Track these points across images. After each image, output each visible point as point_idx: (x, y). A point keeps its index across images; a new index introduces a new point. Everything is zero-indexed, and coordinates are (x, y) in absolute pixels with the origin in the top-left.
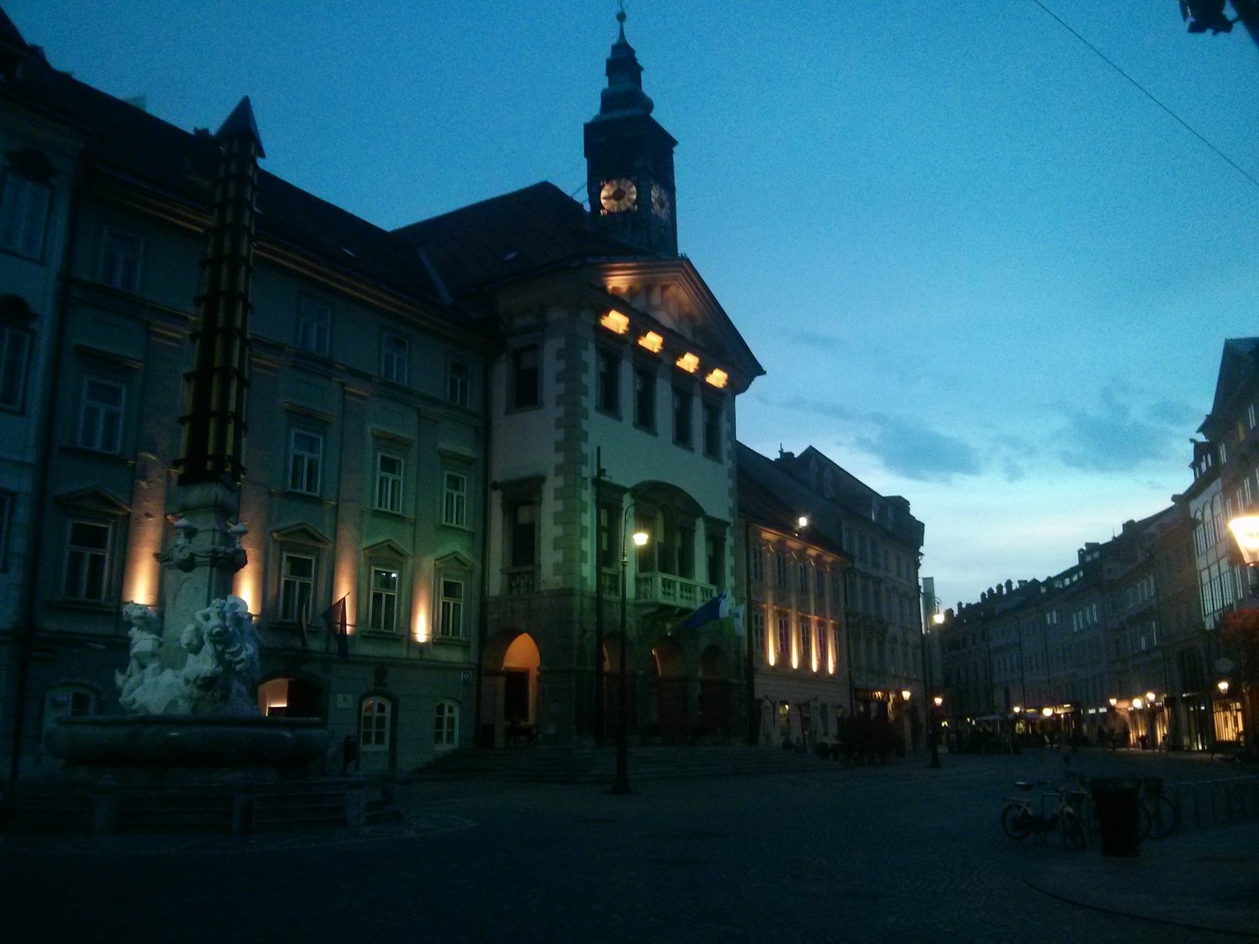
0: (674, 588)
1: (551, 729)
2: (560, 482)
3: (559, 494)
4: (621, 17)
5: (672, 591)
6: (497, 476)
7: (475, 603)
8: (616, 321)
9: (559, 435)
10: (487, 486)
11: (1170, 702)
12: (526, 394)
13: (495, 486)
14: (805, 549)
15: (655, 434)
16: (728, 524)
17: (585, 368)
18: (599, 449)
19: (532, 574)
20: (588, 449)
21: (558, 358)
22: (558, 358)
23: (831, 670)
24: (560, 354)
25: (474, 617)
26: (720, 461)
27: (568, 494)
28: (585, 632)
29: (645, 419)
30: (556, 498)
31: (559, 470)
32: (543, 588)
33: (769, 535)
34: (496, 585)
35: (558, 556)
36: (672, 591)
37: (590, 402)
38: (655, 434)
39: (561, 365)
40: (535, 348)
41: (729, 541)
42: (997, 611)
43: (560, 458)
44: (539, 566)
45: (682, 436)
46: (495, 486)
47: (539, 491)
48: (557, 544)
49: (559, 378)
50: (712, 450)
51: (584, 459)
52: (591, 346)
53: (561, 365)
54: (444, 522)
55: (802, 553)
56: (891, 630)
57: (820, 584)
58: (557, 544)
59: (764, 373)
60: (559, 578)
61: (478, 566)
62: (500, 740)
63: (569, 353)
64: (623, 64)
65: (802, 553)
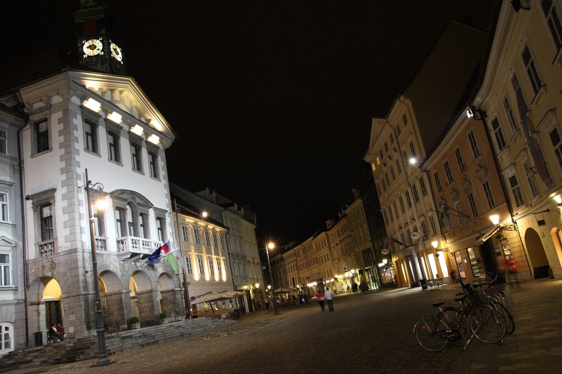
0: (139, 244)
1: (71, 330)
2: (64, 190)
3: (64, 197)
5: (137, 246)
6: (29, 191)
7: (20, 265)
8: (93, 105)
10: (23, 198)
11: (361, 272)
12: (43, 144)
13: (28, 198)
14: (207, 226)
15: (122, 166)
16: (166, 211)
17: (76, 128)
18: (86, 169)
19: (52, 244)
20: (80, 171)
21: (59, 123)
22: (59, 123)
23: (224, 279)
25: (20, 272)
26: (160, 181)
27: (69, 196)
28: (87, 272)
29: (116, 157)
31: (64, 184)
33: (190, 220)
34: (32, 253)
35: (67, 232)
36: (137, 246)
37: (80, 145)
38: (122, 166)
40: (45, 120)
41: (169, 220)
42: (286, 249)
45: (138, 167)
47: (53, 197)
49: (60, 133)
50: (155, 175)
51: (78, 176)
52: (79, 117)
53: (61, 127)
55: (206, 228)
56: (248, 259)
57: (215, 240)
60: (69, 243)
61: (21, 244)
62: (45, 341)
63: (66, 120)
65: (206, 228)
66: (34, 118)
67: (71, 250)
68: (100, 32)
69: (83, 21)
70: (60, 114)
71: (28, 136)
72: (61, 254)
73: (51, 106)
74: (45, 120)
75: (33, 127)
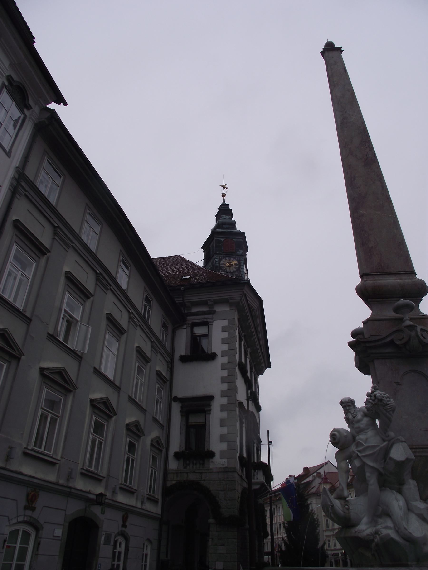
2: (225, 400)
3: (223, 408)
4: (224, 195)
9: (225, 373)
24: (224, 329)
30: (222, 410)
31: (223, 394)
39: (225, 335)
43: (225, 387)
46: (176, 399)
47: (210, 406)
49: (224, 341)
53: (225, 335)
54: (155, 416)
59: (270, 367)
60: (225, 461)
66: (191, 319)
67: (227, 468)
68: (238, 252)
70: (225, 323)
72: (214, 471)
74: (206, 324)
75: (189, 328)
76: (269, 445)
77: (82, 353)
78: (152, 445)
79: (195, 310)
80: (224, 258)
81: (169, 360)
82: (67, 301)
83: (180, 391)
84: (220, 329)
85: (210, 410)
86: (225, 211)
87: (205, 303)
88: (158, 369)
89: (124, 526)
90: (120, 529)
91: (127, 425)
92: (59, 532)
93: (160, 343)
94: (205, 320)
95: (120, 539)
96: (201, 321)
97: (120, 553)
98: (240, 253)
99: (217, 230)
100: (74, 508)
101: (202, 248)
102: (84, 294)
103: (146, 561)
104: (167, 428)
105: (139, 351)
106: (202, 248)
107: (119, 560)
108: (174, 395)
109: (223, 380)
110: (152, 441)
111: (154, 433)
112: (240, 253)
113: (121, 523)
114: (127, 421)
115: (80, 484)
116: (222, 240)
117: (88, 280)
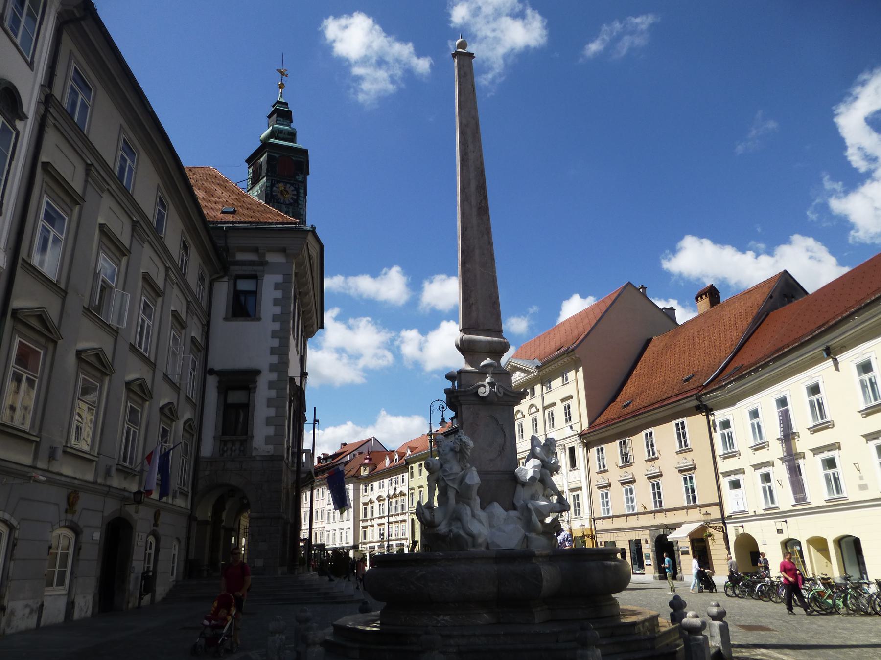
2: (274, 376)
3: (271, 385)
9: (276, 343)
19: (246, 440)
24: (277, 286)
31: (273, 368)
32: (254, 454)
34: (208, 448)
35: (271, 431)
39: (279, 294)
43: (275, 359)
44: (252, 437)
46: (212, 372)
48: (269, 421)
49: (276, 302)
53: (279, 294)
58: (269, 421)
64: (282, 113)
66: (236, 270)
67: (272, 455)
69: (277, 156)
70: (279, 278)
71: (222, 291)
72: (258, 458)
73: (267, 262)
74: (255, 277)
75: (232, 281)
76: (314, 424)
77: (118, 328)
78: (184, 428)
79: (240, 256)
80: (278, 182)
81: (205, 322)
82: (105, 265)
83: (218, 361)
84: (273, 287)
85: (255, 388)
86: (282, 113)
87: (256, 250)
88: (193, 335)
89: (156, 525)
90: (153, 528)
91: (162, 409)
92: (97, 536)
93: (196, 300)
94: (253, 273)
95: (151, 539)
96: (248, 273)
97: (150, 554)
98: (300, 178)
99: (272, 140)
100: (111, 507)
101: (248, 161)
102: (119, 250)
103: (173, 563)
104: (200, 408)
105: (175, 315)
106: (248, 161)
107: (149, 563)
108: (209, 366)
109: (273, 351)
110: (185, 424)
111: (187, 414)
112: (300, 178)
113: (153, 522)
114: (162, 403)
115: (116, 482)
116: (277, 156)
117: (122, 231)
